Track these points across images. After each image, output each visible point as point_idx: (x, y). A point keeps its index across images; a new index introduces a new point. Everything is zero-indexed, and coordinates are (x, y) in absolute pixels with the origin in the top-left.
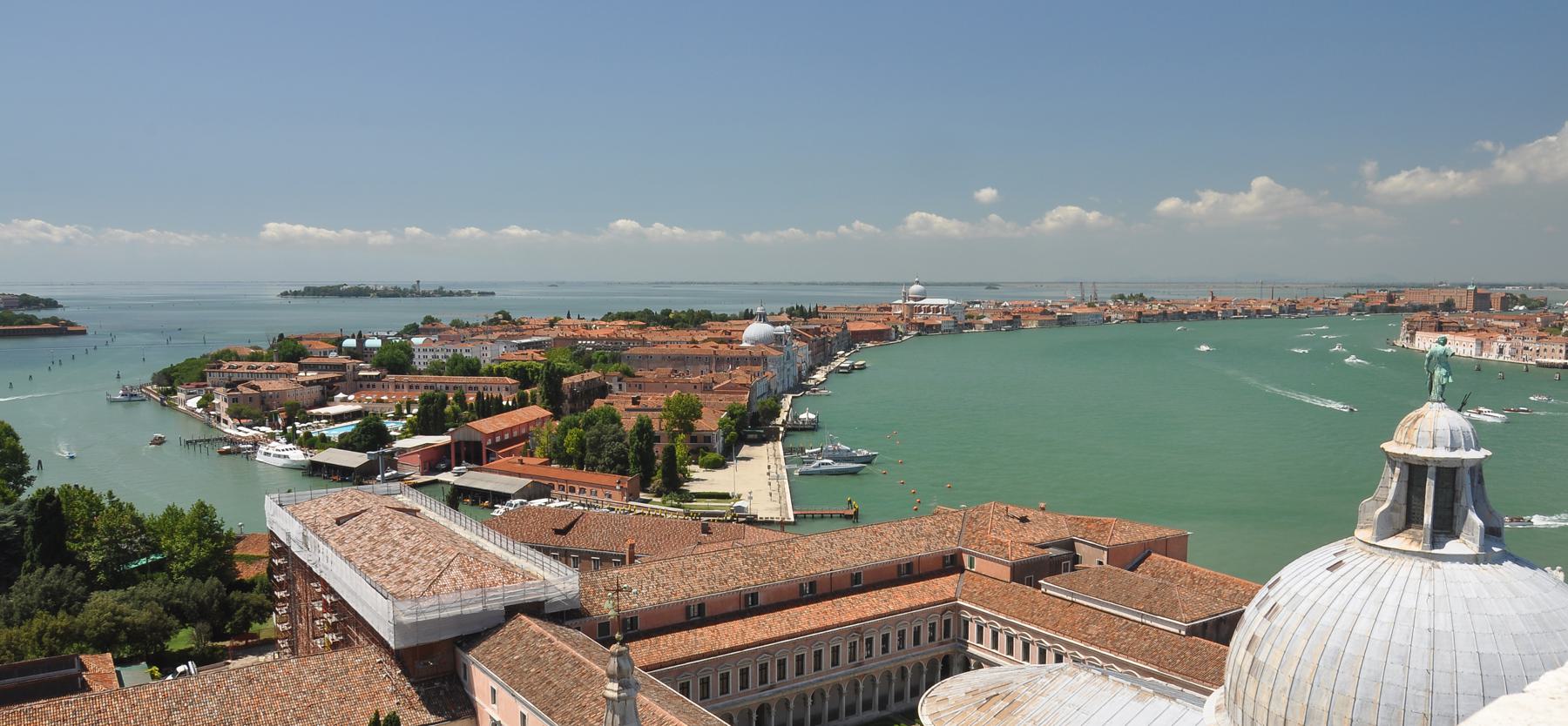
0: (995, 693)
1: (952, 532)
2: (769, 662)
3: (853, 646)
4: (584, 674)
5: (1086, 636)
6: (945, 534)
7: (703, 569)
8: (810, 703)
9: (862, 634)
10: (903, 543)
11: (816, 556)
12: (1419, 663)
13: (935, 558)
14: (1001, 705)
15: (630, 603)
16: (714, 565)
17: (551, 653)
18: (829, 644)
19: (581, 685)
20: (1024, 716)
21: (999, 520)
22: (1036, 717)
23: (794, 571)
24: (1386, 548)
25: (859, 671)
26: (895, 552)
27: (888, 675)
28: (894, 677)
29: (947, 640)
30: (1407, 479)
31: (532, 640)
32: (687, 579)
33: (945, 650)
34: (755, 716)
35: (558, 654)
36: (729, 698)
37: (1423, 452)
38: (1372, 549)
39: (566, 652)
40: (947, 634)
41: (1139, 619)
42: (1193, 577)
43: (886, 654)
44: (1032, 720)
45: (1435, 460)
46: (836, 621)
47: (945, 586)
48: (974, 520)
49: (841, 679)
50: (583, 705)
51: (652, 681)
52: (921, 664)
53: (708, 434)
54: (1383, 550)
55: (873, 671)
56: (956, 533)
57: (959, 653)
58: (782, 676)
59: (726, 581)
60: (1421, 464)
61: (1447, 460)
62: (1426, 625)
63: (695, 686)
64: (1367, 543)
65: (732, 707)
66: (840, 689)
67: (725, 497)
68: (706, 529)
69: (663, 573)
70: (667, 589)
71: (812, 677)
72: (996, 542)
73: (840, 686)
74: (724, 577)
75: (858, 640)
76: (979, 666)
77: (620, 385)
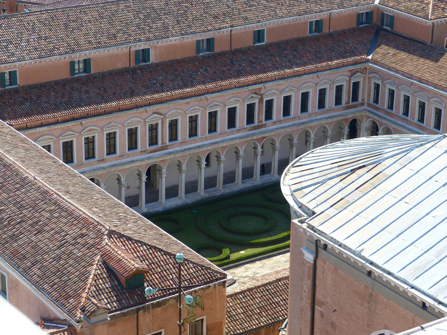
2: (160, 122)
3: (251, 108)
7: (90, 22)
8: (203, 166)
9: (262, 95)
11: (215, 11)
15: (8, 57)
16: (102, 18)
18: (225, 105)
23: (190, 26)
25: (257, 134)
28: (295, 141)
29: (355, 103)
32: (72, 32)
33: (351, 114)
34: (144, 177)
36: (116, 159)
40: (355, 97)
43: (287, 117)
49: (238, 142)
51: (23, 141)
55: (273, 134)
58: (173, 137)
59: (115, 36)
65: (121, 168)
66: (237, 153)
69: (45, 25)
70: (49, 43)
71: (206, 139)
73: (237, 148)
74: (113, 31)
75: (256, 101)
76: (388, 132)
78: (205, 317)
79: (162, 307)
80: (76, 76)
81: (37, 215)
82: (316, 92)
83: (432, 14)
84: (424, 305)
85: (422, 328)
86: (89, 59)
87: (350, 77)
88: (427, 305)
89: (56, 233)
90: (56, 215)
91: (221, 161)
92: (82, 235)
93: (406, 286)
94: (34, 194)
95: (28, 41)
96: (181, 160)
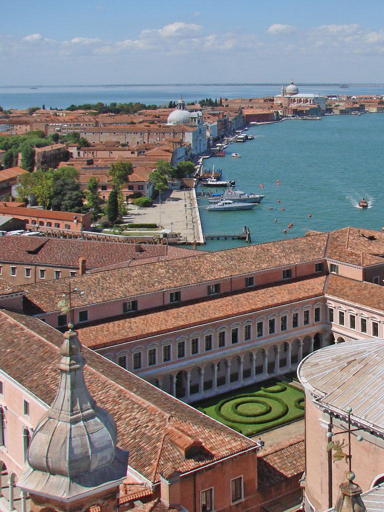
0: (353, 359)
1: (320, 248)
4: (47, 353)
6: (315, 249)
7: (136, 277)
10: (284, 256)
13: (309, 265)
14: (358, 367)
17: (23, 338)
18: (230, 328)
19: (45, 360)
20: (374, 374)
21: (353, 239)
26: (278, 263)
27: (275, 348)
28: (279, 350)
31: (9, 329)
35: (28, 339)
39: (34, 336)
44: (380, 377)
46: (235, 311)
47: (316, 285)
48: (335, 239)
50: (46, 374)
51: (98, 357)
52: (299, 340)
53: (141, 184)
56: (323, 248)
57: (326, 331)
63: (130, 360)
67: (154, 226)
68: (141, 250)
70: (110, 291)
72: (352, 254)
74: (152, 282)
77: (79, 153)
78: (242, 476)
79: (212, 470)
80: (127, 312)
81: (116, 407)
82: (290, 315)
86: (137, 301)
87: (314, 304)
89: (131, 420)
90: (130, 407)
91: (240, 362)
92: (151, 420)
94: (113, 393)
95: (95, 291)
96: (200, 367)
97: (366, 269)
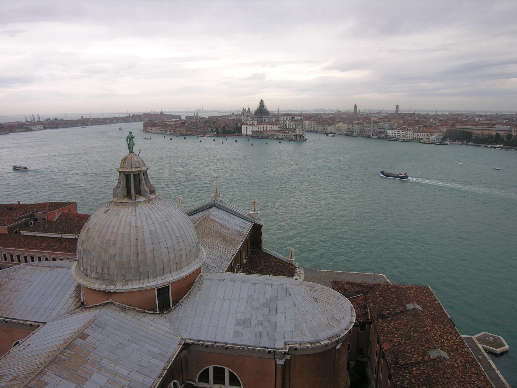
5: (41, 247)
12: (133, 237)
22: (11, 288)
24: (122, 203)
30: (125, 179)
37: (128, 170)
38: (118, 204)
41: (60, 236)
42: (80, 217)
44: (9, 290)
45: (132, 172)
54: (121, 203)
60: (129, 174)
61: (136, 171)
62: (134, 225)
64: (116, 202)
83: (7, 224)
84: (31, 325)
85: (33, 334)
88: (32, 325)
93: (22, 321)
97: (9, 227)
